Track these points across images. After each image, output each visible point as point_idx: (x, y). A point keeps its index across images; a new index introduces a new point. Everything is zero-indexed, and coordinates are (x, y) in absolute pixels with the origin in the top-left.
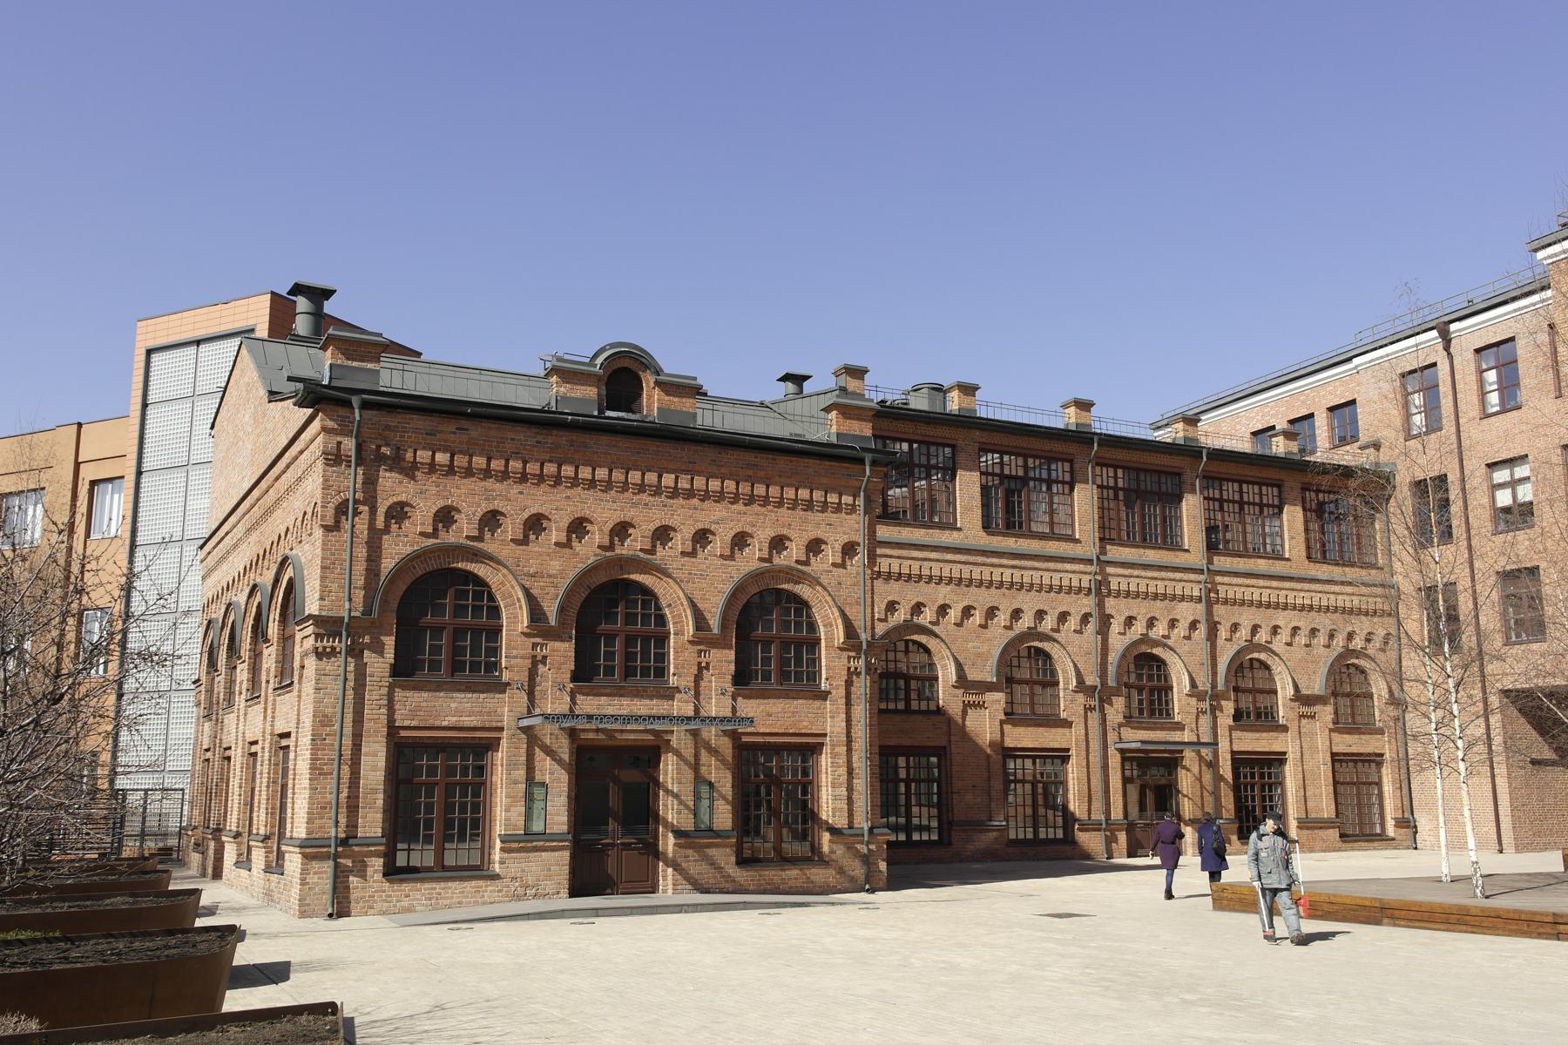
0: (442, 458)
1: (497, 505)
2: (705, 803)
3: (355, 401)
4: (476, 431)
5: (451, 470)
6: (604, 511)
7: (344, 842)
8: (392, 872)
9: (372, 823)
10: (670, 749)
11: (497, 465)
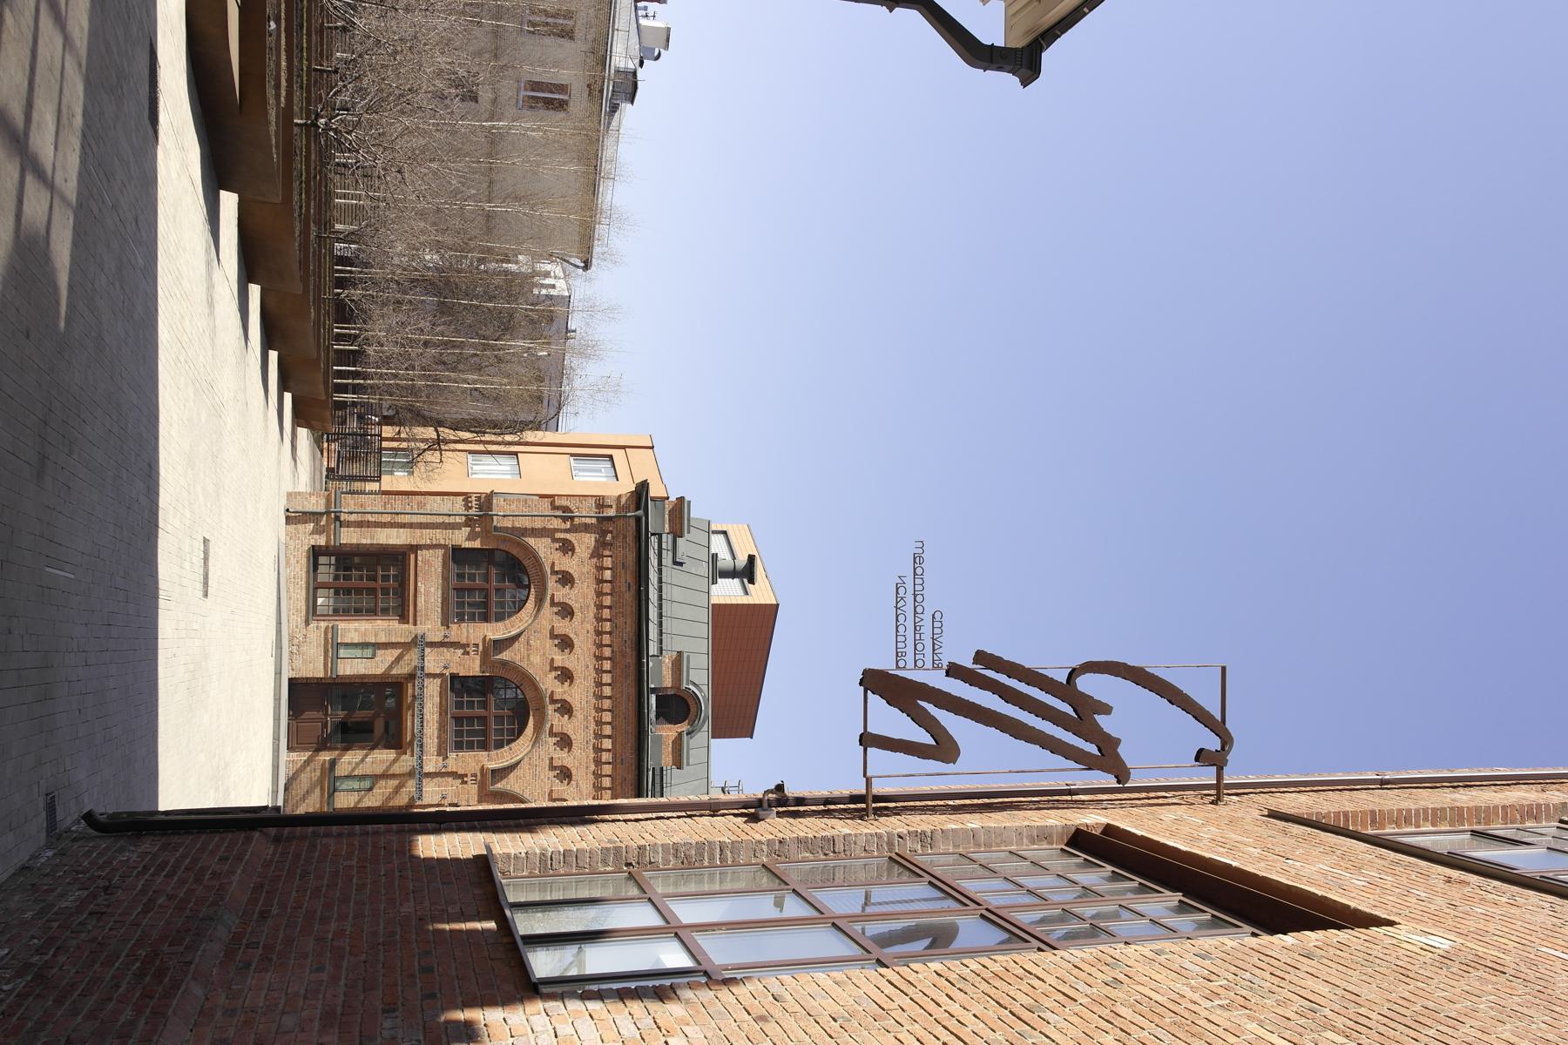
0: (608, 575)
1: (578, 615)
2: (356, 785)
3: (641, 512)
4: (629, 597)
5: (600, 581)
6: (580, 694)
7: (337, 518)
8: (316, 553)
9: (349, 537)
10: (399, 755)
11: (606, 613)
